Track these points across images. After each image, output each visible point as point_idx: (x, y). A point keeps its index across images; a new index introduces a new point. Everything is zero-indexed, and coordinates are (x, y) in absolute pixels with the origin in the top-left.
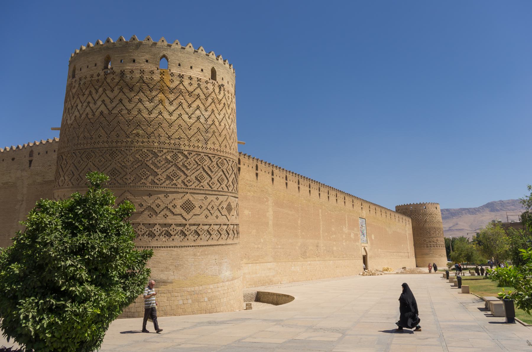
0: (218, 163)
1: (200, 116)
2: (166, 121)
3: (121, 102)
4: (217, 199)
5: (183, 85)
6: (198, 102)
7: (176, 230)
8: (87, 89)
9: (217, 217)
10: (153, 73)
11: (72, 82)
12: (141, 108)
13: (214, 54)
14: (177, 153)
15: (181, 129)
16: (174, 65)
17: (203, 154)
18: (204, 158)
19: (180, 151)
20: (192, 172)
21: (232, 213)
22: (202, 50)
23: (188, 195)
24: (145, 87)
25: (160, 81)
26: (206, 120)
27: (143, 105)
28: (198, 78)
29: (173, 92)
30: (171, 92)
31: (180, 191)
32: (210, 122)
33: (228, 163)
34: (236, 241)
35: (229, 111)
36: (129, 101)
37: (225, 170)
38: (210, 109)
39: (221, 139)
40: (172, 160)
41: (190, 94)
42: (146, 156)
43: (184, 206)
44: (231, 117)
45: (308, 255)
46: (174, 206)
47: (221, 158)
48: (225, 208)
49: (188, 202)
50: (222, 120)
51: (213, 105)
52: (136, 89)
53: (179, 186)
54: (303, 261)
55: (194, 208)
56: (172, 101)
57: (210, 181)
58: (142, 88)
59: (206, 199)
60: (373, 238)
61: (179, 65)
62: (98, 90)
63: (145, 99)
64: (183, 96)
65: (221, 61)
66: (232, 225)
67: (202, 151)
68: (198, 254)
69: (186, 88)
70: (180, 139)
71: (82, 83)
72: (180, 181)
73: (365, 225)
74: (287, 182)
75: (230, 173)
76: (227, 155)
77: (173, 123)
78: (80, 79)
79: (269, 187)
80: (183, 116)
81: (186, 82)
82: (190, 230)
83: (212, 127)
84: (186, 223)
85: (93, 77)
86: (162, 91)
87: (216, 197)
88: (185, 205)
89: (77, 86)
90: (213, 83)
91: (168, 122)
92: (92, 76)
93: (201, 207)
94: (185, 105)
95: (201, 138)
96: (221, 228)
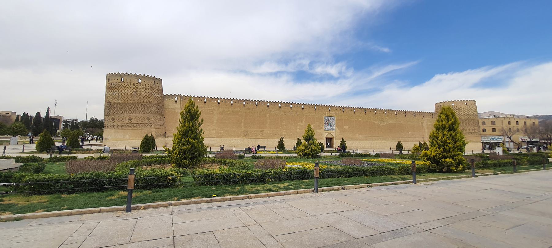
4: (124, 116)
26: (118, 94)
32: (120, 94)
38: (120, 91)
39: (124, 99)
41: (114, 87)
49: (113, 118)
51: (122, 89)
93: (117, 119)
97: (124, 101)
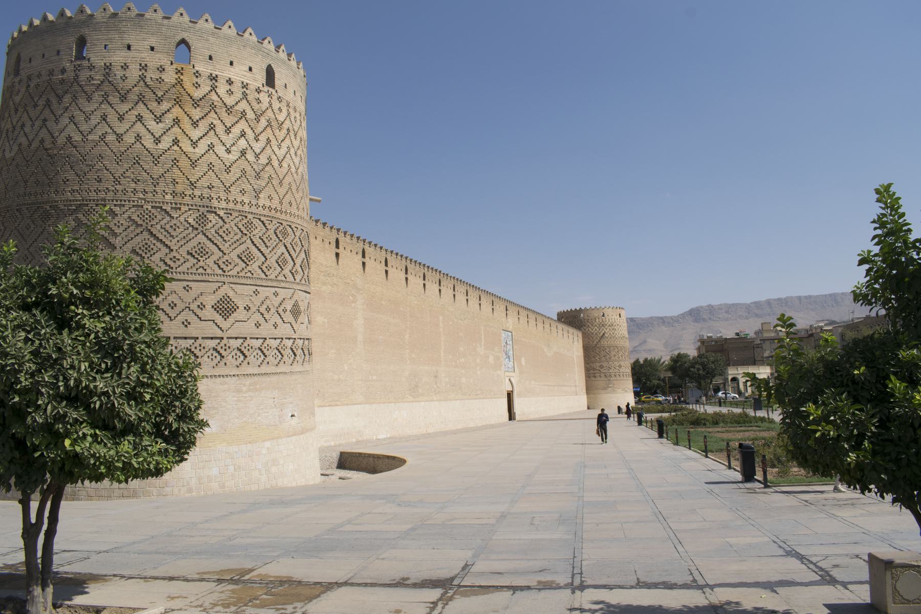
0: (278, 232)
1: (247, 149)
2: (187, 155)
3: (104, 119)
4: (276, 294)
5: (217, 94)
6: (242, 125)
7: (204, 348)
8: (41, 96)
9: (275, 326)
10: (164, 70)
11: (14, 82)
12: (142, 131)
13: (271, 43)
14: (205, 214)
15: (213, 170)
16: (201, 57)
17: (251, 215)
18: (254, 223)
19: (211, 210)
20: (233, 247)
21: (300, 320)
22: (251, 34)
23: (225, 287)
24: (149, 95)
25: (176, 84)
26: (257, 156)
27: (145, 126)
28: (243, 83)
29: (198, 105)
30: (195, 105)
31: (211, 280)
32: (263, 160)
33: (294, 233)
34: (307, 367)
35: (296, 143)
36: (118, 119)
37: (289, 246)
38: (263, 138)
40: (196, 226)
41: (229, 110)
42: (150, 216)
43: (218, 307)
44: (299, 152)
45: (420, 391)
46: (202, 307)
47: (282, 224)
48: (288, 311)
49: (227, 300)
50: (284, 157)
51: (269, 130)
52: (133, 97)
53: (209, 271)
54: (412, 402)
55: (235, 310)
56: (198, 121)
57: (263, 263)
58: (144, 97)
59: (256, 295)
60: (523, 363)
61: (211, 58)
62: (62, 97)
63: (147, 115)
64: (216, 113)
65: (283, 55)
66: (300, 339)
67: (250, 211)
68: (244, 389)
69: (221, 99)
70: (210, 188)
71: (32, 85)
72: (210, 261)
73: (511, 342)
74: (387, 269)
75: (298, 249)
76: (292, 219)
77: (198, 160)
78: (29, 78)
79: (357, 277)
80: (216, 149)
81: (222, 89)
82: (229, 347)
83: (267, 169)
84: (222, 336)
85: (53, 75)
86: (178, 102)
87: (273, 290)
88: (221, 305)
89: (23, 90)
90: (270, 92)
91: (189, 158)
92: (51, 73)
93: (247, 309)
94: (220, 129)
95: (247, 187)
96: (282, 345)
97: (281, 203)
